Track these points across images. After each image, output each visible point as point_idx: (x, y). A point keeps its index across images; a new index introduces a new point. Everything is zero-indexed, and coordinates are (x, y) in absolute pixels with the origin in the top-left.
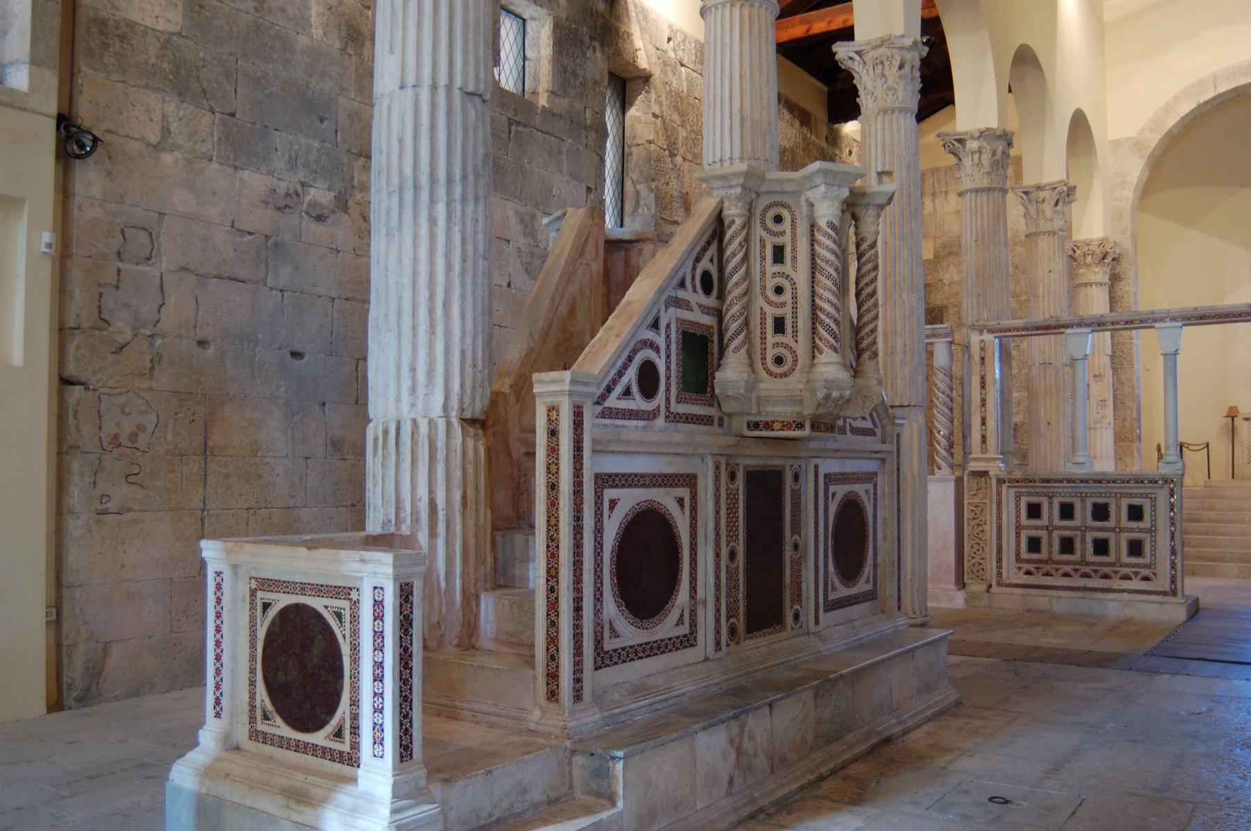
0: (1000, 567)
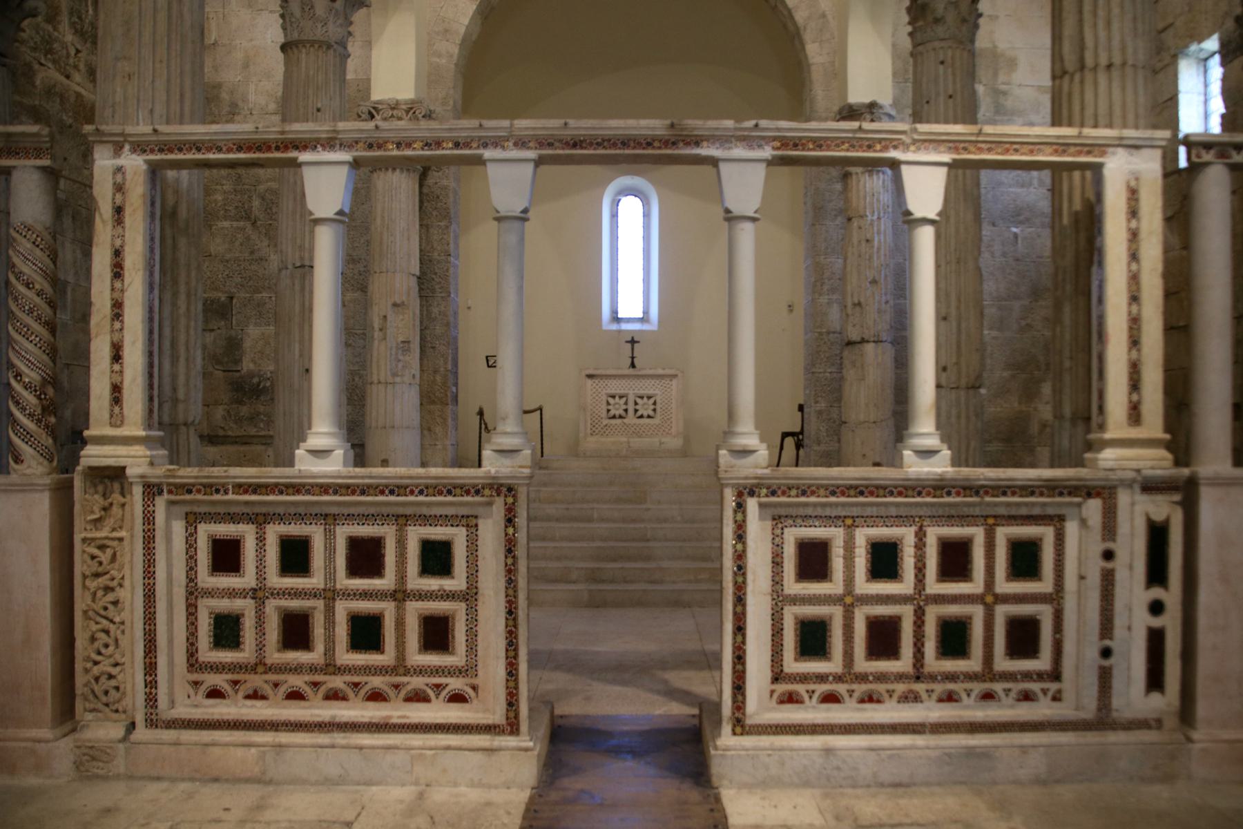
0: (151, 684)
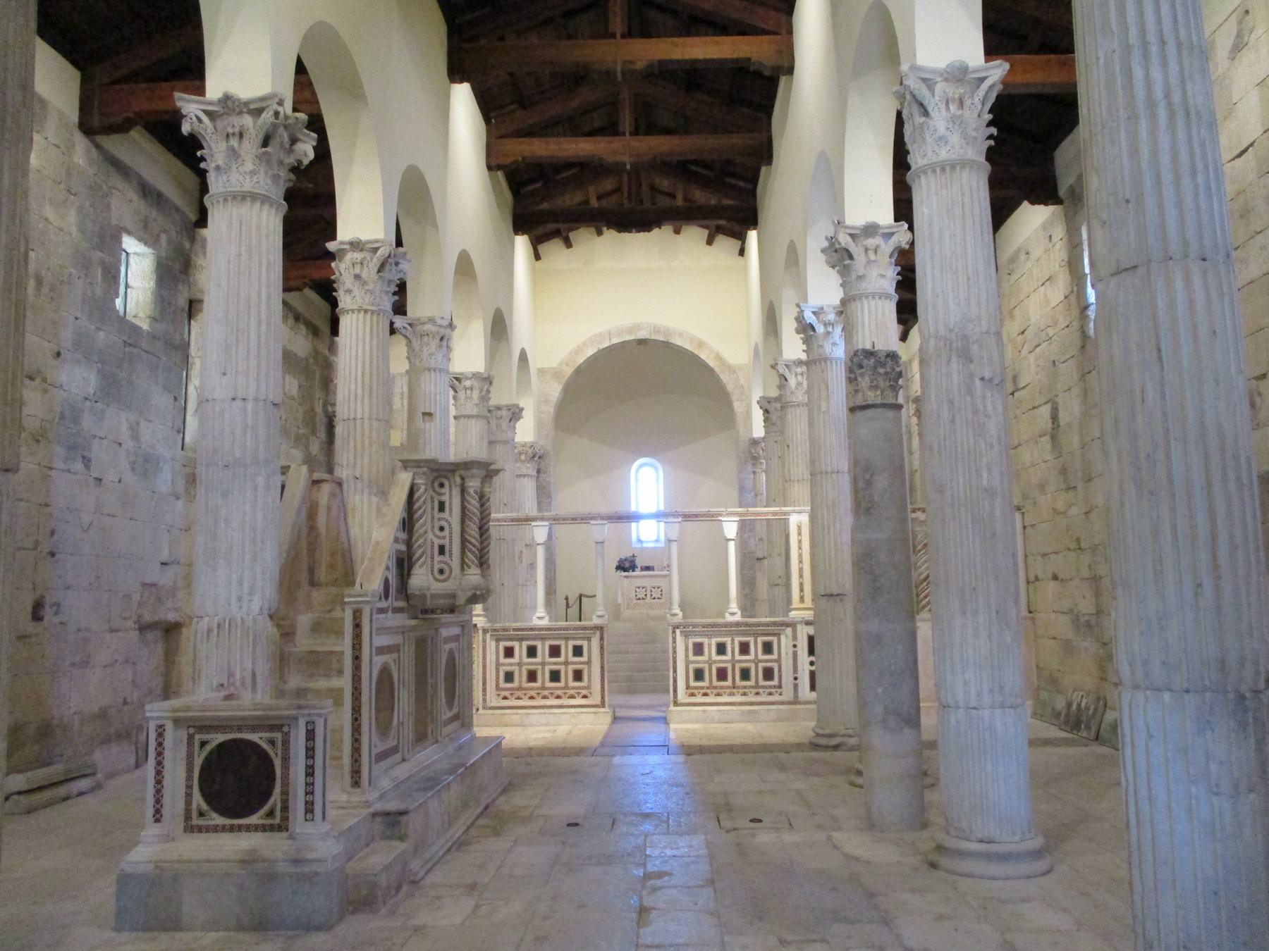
0: (484, 695)
